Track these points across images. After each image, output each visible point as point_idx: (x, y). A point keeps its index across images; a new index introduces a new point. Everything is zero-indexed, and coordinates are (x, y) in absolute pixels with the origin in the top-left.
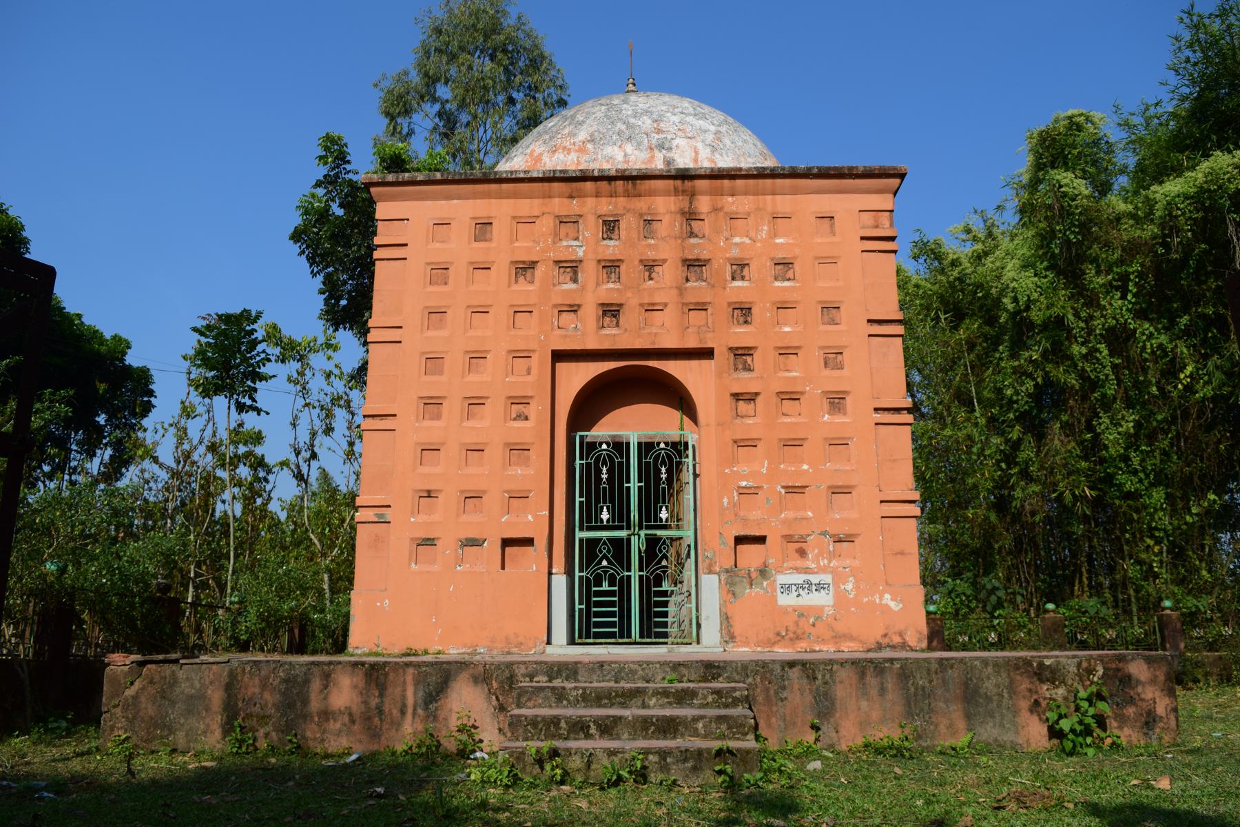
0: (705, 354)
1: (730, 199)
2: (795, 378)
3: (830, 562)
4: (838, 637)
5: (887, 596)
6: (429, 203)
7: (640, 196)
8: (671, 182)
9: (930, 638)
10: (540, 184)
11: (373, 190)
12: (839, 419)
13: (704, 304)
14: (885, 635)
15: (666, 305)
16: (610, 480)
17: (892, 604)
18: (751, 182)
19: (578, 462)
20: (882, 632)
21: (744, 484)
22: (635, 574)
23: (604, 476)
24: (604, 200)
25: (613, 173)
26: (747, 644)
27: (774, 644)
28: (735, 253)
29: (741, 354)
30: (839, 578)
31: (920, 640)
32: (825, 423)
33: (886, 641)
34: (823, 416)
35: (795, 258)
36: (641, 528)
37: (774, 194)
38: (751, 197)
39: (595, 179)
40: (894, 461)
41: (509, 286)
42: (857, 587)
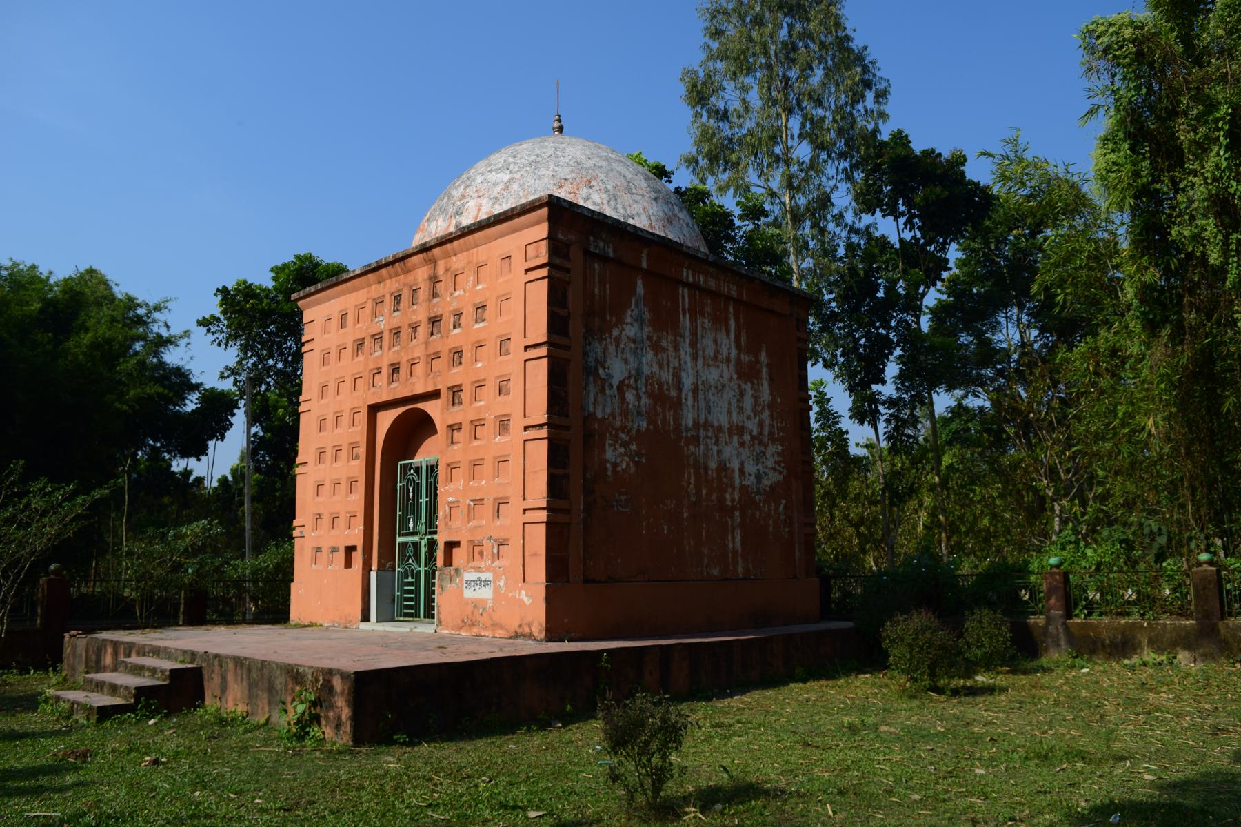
0: (435, 395)
1: (454, 258)
2: (480, 407)
3: (492, 563)
4: (496, 625)
5: (523, 592)
6: (323, 305)
7: (409, 271)
8: (420, 256)
9: (548, 630)
10: (361, 278)
11: (300, 303)
12: (506, 439)
13: (438, 353)
14: (520, 626)
15: (419, 358)
16: (413, 496)
17: (526, 599)
18: (461, 240)
19: (399, 485)
20: (517, 623)
21: (450, 499)
22: (422, 569)
23: (411, 494)
24: (388, 282)
25: (391, 259)
26: (447, 628)
27: (461, 628)
28: (455, 305)
29: (455, 390)
30: (496, 578)
31: (540, 632)
32: (496, 443)
33: (520, 630)
34: (495, 438)
35: (486, 300)
36: (426, 534)
37: (477, 247)
38: (465, 253)
39: (386, 265)
40: (536, 472)
41: (353, 359)
42: (506, 584)
